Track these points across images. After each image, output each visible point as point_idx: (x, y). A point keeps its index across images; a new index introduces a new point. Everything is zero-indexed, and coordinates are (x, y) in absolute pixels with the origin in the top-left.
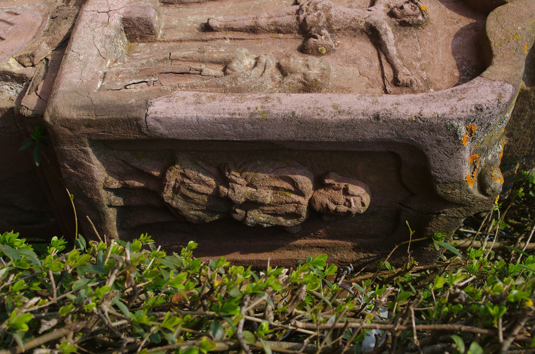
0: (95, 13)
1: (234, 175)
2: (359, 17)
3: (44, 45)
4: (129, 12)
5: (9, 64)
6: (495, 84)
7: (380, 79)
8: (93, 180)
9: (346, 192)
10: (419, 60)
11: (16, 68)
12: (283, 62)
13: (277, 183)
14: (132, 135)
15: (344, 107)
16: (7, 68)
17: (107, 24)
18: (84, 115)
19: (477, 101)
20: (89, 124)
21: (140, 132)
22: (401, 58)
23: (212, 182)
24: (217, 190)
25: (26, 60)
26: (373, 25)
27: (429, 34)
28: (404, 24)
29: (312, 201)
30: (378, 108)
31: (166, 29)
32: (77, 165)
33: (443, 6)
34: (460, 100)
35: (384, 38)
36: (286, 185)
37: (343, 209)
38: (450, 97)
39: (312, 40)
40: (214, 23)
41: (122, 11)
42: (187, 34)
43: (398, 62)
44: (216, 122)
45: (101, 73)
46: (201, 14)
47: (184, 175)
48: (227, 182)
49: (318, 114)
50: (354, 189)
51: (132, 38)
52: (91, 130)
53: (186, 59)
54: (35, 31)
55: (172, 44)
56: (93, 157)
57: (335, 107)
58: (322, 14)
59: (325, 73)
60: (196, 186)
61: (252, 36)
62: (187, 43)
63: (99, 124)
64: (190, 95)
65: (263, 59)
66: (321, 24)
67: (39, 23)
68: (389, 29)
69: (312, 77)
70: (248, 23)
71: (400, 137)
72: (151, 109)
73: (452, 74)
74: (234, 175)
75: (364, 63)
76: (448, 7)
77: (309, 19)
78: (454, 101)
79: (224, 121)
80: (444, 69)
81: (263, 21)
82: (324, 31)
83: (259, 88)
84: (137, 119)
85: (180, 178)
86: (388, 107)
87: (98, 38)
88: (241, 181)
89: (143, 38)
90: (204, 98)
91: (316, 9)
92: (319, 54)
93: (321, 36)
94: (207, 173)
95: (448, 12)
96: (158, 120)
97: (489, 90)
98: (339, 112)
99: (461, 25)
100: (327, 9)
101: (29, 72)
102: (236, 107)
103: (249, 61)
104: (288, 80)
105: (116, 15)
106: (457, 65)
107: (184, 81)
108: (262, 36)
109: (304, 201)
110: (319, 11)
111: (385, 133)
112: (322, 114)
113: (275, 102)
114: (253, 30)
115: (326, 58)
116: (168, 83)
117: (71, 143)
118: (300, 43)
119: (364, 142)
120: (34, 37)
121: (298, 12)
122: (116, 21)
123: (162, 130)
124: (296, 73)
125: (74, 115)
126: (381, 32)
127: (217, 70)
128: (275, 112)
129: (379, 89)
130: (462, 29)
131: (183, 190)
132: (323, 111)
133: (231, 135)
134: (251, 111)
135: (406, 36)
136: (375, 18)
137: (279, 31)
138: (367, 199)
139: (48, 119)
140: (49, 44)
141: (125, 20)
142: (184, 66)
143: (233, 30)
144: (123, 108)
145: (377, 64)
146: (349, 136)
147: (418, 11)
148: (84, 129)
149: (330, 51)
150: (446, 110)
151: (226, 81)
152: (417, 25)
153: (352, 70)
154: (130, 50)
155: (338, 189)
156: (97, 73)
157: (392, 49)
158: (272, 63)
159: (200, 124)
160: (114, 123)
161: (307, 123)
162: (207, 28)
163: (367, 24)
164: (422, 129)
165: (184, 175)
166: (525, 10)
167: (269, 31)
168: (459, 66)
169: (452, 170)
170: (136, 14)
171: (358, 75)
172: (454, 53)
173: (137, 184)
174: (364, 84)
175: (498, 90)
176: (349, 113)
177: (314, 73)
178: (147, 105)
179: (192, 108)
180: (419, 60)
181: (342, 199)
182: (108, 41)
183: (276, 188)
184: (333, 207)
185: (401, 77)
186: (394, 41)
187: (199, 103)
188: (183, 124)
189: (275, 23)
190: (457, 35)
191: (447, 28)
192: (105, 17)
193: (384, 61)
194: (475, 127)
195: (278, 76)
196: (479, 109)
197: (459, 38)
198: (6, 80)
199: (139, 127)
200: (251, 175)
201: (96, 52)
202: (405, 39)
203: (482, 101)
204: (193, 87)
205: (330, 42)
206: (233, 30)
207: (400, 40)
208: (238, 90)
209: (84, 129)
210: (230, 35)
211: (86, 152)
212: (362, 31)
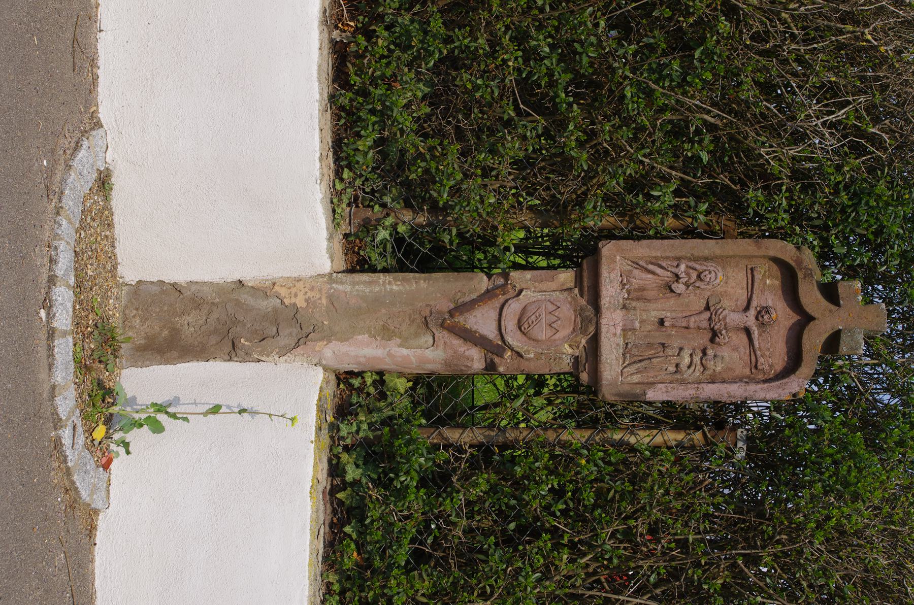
15: (732, 394)
17: (615, 335)
35: (753, 336)
38: (779, 388)
41: (621, 324)
43: (758, 353)
54: (573, 323)
57: (728, 393)
75: (742, 350)
76: (788, 305)
86: (751, 393)
95: (788, 309)
113: (701, 391)
115: (724, 347)
130: (793, 324)
135: (764, 331)
136: (748, 323)
145: (748, 351)
150: (776, 395)
153: (736, 355)
168: (788, 353)
172: (787, 343)
178: (645, 394)
180: (769, 350)
190: (790, 329)
192: (612, 329)
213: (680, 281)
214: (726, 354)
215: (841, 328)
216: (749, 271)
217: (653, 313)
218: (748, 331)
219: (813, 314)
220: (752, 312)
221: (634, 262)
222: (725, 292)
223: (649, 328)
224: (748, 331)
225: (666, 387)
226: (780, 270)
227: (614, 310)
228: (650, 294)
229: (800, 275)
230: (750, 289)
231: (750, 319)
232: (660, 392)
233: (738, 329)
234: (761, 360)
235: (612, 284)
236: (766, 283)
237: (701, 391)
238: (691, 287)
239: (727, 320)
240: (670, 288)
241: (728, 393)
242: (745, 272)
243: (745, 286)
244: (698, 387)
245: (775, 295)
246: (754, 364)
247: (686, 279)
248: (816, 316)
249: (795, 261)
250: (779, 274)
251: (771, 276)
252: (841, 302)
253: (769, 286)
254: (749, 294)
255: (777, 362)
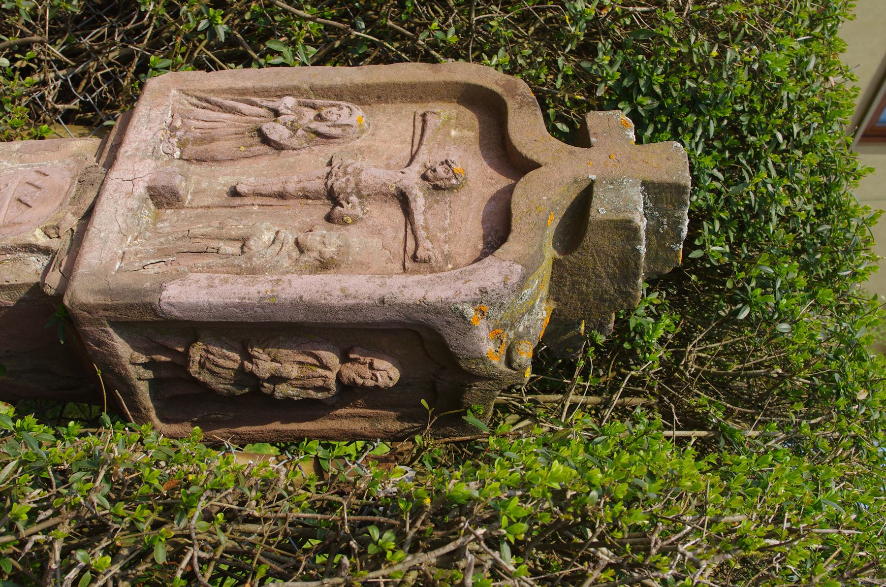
0: (119, 181)
1: (257, 352)
2: (390, 181)
3: (70, 216)
4: (154, 180)
5: (34, 236)
6: (504, 264)
7: (402, 252)
8: (117, 356)
9: (371, 366)
10: (444, 230)
11: (41, 240)
12: (302, 237)
13: (302, 358)
14: (149, 317)
15: (352, 291)
16: (32, 240)
17: (130, 194)
18: (100, 300)
19: (482, 283)
20: (106, 308)
21: (156, 315)
22: (426, 228)
23: (237, 357)
24: (242, 364)
25: (52, 232)
26: (404, 190)
27: (463, 198)
28: (436, 188)
29: (339, 375)
30: (384, 292)
31: (195, 193)
32: (100, 343)
33: (485, 164)
34: (466, 282)
35: (412, 205)
36: (311, 360)
37: (370, 383)
38: (457, 279)
39: (339, 208)
40: (241, 188)
41: (147, 179)
42: (216, 199)
43: (421, 233)
44: (226, 306)
45: (120, 252)
46: (234, 174)
47: (207, 351)
48: (250, 358)
49: (325, 299)
50: (378, 363)
51: (159, 205)
52: (108, 313)
53: (205, 236)
54: (62, 196)
55: (200, 211)
56: (115, 336)
57: (342, 290)
58: (351, 179)
59: (345, 249)
60: (221, 362)
61: (281, 202)
62: (215, 210)
63: (116, 308)
64: (203, 277)
65: (282, 236)
66: (349, 191)
67: (67, 187)
68: (420, 194)
69: (328, 256)
70: (277, 188)
71: (409, 319)
72: (164, 293)
73: (475, 247)
74: (257, 352)
75: (390, 232)
76: (491, 165)
77: (337, 185)
78: (459, 284)
79: (235, 306)
80: (469, 241)
81: (291, 187)
82: (354, 199)
83: (274, 268)
84: (151, 304)
85: (204, 353)
86: (395, 290)
87: (121, 212)
88: (265, 356)
89: (170, 205)
90: (216, 281)
91: (345, 174)
92: (345, 223)
93: (348, 203)
94: (231, 349)
95: (490, 171)
96: (171, 305)
97: (497, 270)
98: (346, 296)
99: (499, 187)
100: (358, 173)
101: (55, 244)
102: (247, 291)
103: (268, 237)
104: (305, 258)
105: (141, 183)
106: (484, 235)
107: (202, 261)
108: (291, 202)
109: (332, 376)
110: (348, 176)
111: (392, 315)
112: (329, 298)
113: (286, 285)
114: (282, 196)
115: (353, 229)
116: (185, 262)
117: (91, 324)
118: (328, 209)
119: (378, 324)
120: (61, 205)
121: (329, 175)
122: (140, 190)
123: (176, 313)
124: (312, 250)
125: (91, 299)
126: (411, 198)
127: (232, 248)
128: (284, 296)
129: (398, 266)
130: (498, 192)
131: (208, 365)
132: (330, 295)
133: (244, 317)
134: (261, 295)
135: (437, 202)
136: (406, 182)
137: (308, 198)
138: (395, 374)
139: (67, 303)
140: (74, 214)
141: (149, 188)
142: (200, 245)
143: (261, 195)
144: (138, 293)
146: (359, 318)
147: (451, 174)
148: (101, 312)
149: (356, 220)
150: (450, 293)
151: (241, 261)
152: (451, 189)
153: (375, 242)
154: (157, 219)
155: (364, 364)
156: (116, 253)
157: (419, 219)
158: (291, 240)
159: (211, 307)
160: (130, 307)
161: (314, 307)
162: (235, 193)
163: (397, 188)
164: (428, 312)
165: (207, 351)
166: (557, 176)
167: (298, 197)
168: (485, 237)
169: (469, 347)
170: (160, 183)
171: (381, 247)
172: (483, 222)
173: (163, 358)
174: (384, 259)
175: (505, 271)
176: (355, 297)
177: (330, 251)
178: (161, 289)
179: (204, 292)
180: (444, 230)
181: (368, 373)
182: (130, 214)
183: (300, 363)
184: (360, 381)
185: (421, 253)
186: (423, 208)
187: (212, 287)
188: (196, 308)
189: (303, 189)
190: (493, 199)
191: (483, 190)
192: (128, 186)
193: (409, 231)
194: (485, 308)
195: (295, 254)
196: (483, 291)
197: (493, 203)
198: (33, 252)
199: (154, 310)
200: (274, 351)
201: (117, 229)
202: (436, 205)
203: (487, 284)
204: (209, 268)
205: (358, 211)
206: (261, 195)
207: (430, 207)
208: (253, 271)
209: (101, 312)
210: (259, 201)
211: (106, 332)
212: (393, 196)
213: (280, 118)
214: (355, 239)
215: (594, 177)
216: (419, 119)
217: (221, 180)
218: (403, 199)
219: (535, 158)
220: (416, 168)
221: (200, 99)
222: (369, 147)
223: (209, 201)
224: (403, 199)
225: (211, 279)
226: (479, 118)
227: (143, 159)
228: (220, 148)
229: (511, 105)
230: (416, 142)
231: (411, 179)
232: (194, 287)
233: (382, 195)
234: (425, 244)
235: (150, 125)
236: (449, 133)
237: (286, 285)
238: (300, 132)
239: (363, 177)
240: (265, 140)
241: (342, 290)
242: (411, 121)
243: (409, 139)
244: (279, 280)
245: (465, 150)
246: (410, 252)
247: (292, 118)
248: (540, 162)
249: (503, 86)
250: (477, 123)
251: (460, 126)
252: (593, 140)
253: (455, 139)
254: (415, 148)
255: (461, 251)
